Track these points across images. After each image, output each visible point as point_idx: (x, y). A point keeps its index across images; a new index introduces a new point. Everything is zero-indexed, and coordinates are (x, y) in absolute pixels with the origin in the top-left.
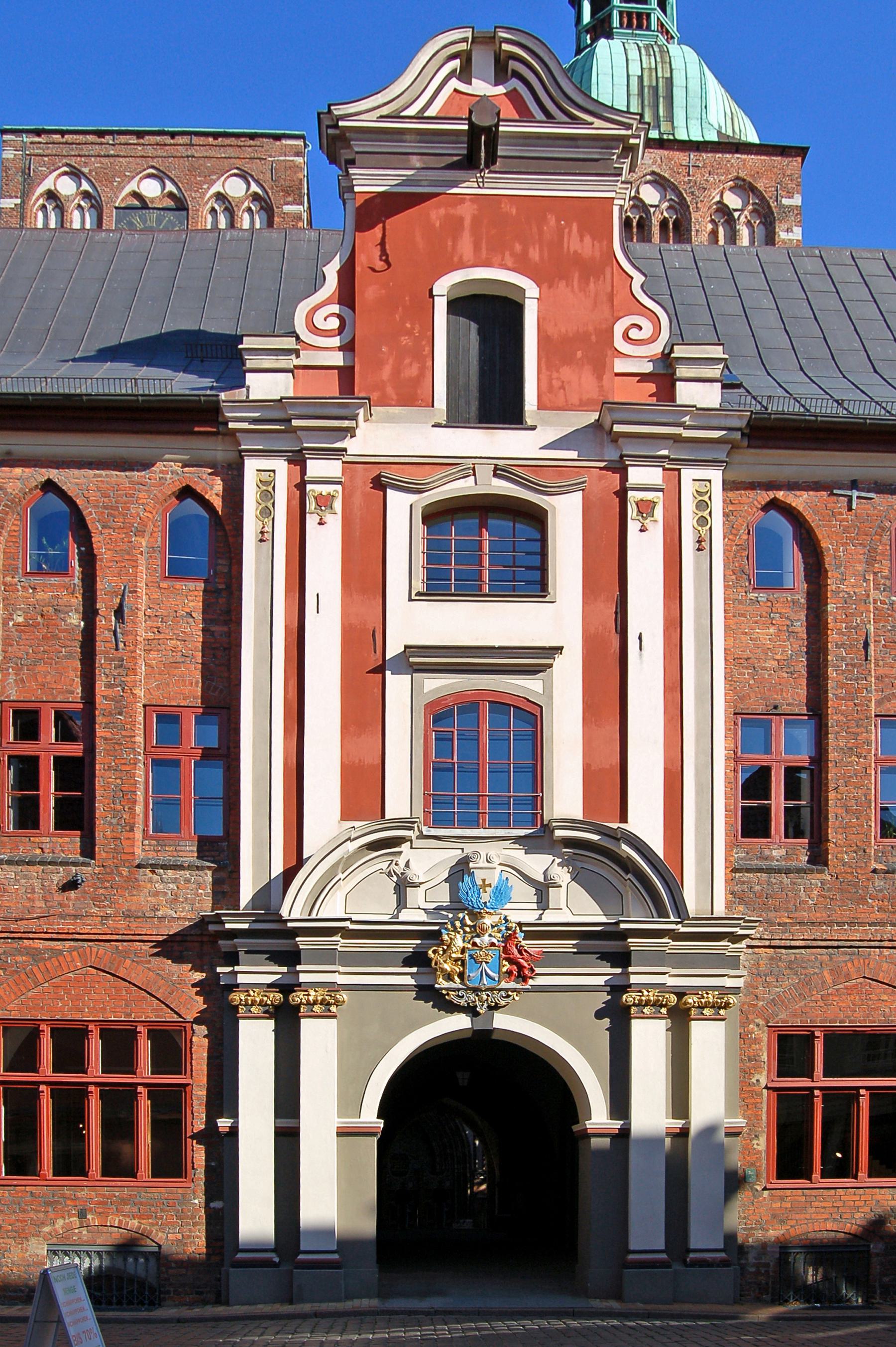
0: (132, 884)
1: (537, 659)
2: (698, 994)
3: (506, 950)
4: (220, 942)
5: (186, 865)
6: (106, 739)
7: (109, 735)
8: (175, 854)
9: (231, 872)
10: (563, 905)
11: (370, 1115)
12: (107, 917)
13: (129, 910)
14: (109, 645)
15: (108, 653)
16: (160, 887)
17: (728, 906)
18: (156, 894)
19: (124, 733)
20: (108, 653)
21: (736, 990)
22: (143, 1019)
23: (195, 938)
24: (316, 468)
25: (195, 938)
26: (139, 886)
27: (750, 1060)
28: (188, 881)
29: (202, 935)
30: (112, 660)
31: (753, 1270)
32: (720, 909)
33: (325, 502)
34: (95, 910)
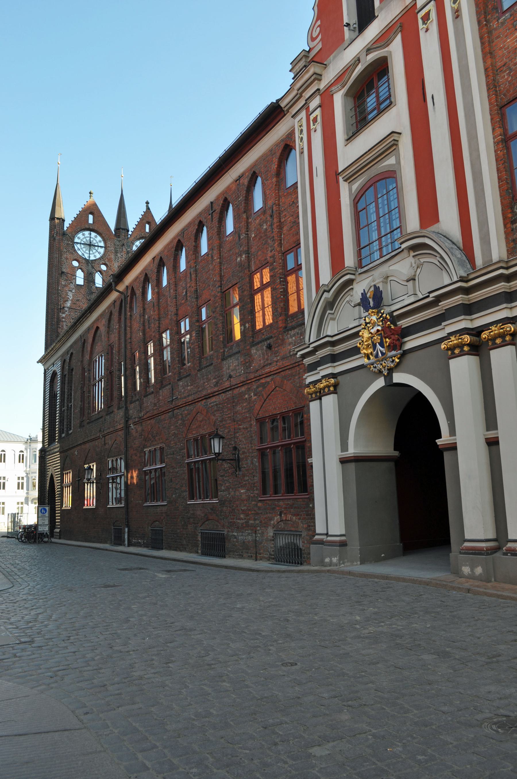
16: (290, 340)
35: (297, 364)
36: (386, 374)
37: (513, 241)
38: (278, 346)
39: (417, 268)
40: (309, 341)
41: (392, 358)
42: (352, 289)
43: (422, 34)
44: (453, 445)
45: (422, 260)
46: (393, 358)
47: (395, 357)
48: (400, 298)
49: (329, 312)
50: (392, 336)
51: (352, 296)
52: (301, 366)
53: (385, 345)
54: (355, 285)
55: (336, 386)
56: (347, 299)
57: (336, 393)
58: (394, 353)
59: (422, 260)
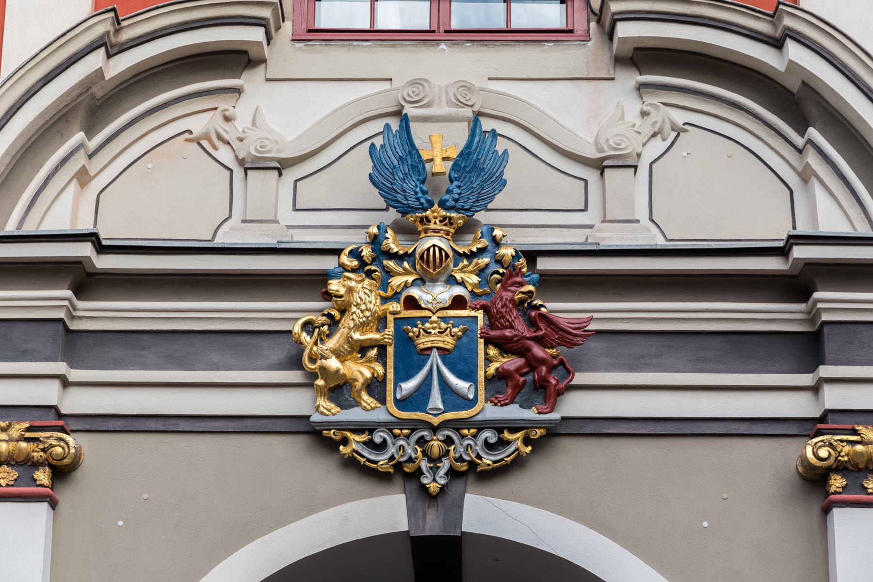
10: (642, 213)
36: (433, 487)
39: (654, 135)
42: (237, 91)
45: (680, 117)
46: (507, 435)
47: (513, 430)
48: (533, 211)
49: (80, 136)
50: (538, 351)
51: (227, 119)
53: (481, 374)
54: (251, 81)
55: (63, 471)
57: (54, 504)
58: (514, 412)
59: (680, 117)
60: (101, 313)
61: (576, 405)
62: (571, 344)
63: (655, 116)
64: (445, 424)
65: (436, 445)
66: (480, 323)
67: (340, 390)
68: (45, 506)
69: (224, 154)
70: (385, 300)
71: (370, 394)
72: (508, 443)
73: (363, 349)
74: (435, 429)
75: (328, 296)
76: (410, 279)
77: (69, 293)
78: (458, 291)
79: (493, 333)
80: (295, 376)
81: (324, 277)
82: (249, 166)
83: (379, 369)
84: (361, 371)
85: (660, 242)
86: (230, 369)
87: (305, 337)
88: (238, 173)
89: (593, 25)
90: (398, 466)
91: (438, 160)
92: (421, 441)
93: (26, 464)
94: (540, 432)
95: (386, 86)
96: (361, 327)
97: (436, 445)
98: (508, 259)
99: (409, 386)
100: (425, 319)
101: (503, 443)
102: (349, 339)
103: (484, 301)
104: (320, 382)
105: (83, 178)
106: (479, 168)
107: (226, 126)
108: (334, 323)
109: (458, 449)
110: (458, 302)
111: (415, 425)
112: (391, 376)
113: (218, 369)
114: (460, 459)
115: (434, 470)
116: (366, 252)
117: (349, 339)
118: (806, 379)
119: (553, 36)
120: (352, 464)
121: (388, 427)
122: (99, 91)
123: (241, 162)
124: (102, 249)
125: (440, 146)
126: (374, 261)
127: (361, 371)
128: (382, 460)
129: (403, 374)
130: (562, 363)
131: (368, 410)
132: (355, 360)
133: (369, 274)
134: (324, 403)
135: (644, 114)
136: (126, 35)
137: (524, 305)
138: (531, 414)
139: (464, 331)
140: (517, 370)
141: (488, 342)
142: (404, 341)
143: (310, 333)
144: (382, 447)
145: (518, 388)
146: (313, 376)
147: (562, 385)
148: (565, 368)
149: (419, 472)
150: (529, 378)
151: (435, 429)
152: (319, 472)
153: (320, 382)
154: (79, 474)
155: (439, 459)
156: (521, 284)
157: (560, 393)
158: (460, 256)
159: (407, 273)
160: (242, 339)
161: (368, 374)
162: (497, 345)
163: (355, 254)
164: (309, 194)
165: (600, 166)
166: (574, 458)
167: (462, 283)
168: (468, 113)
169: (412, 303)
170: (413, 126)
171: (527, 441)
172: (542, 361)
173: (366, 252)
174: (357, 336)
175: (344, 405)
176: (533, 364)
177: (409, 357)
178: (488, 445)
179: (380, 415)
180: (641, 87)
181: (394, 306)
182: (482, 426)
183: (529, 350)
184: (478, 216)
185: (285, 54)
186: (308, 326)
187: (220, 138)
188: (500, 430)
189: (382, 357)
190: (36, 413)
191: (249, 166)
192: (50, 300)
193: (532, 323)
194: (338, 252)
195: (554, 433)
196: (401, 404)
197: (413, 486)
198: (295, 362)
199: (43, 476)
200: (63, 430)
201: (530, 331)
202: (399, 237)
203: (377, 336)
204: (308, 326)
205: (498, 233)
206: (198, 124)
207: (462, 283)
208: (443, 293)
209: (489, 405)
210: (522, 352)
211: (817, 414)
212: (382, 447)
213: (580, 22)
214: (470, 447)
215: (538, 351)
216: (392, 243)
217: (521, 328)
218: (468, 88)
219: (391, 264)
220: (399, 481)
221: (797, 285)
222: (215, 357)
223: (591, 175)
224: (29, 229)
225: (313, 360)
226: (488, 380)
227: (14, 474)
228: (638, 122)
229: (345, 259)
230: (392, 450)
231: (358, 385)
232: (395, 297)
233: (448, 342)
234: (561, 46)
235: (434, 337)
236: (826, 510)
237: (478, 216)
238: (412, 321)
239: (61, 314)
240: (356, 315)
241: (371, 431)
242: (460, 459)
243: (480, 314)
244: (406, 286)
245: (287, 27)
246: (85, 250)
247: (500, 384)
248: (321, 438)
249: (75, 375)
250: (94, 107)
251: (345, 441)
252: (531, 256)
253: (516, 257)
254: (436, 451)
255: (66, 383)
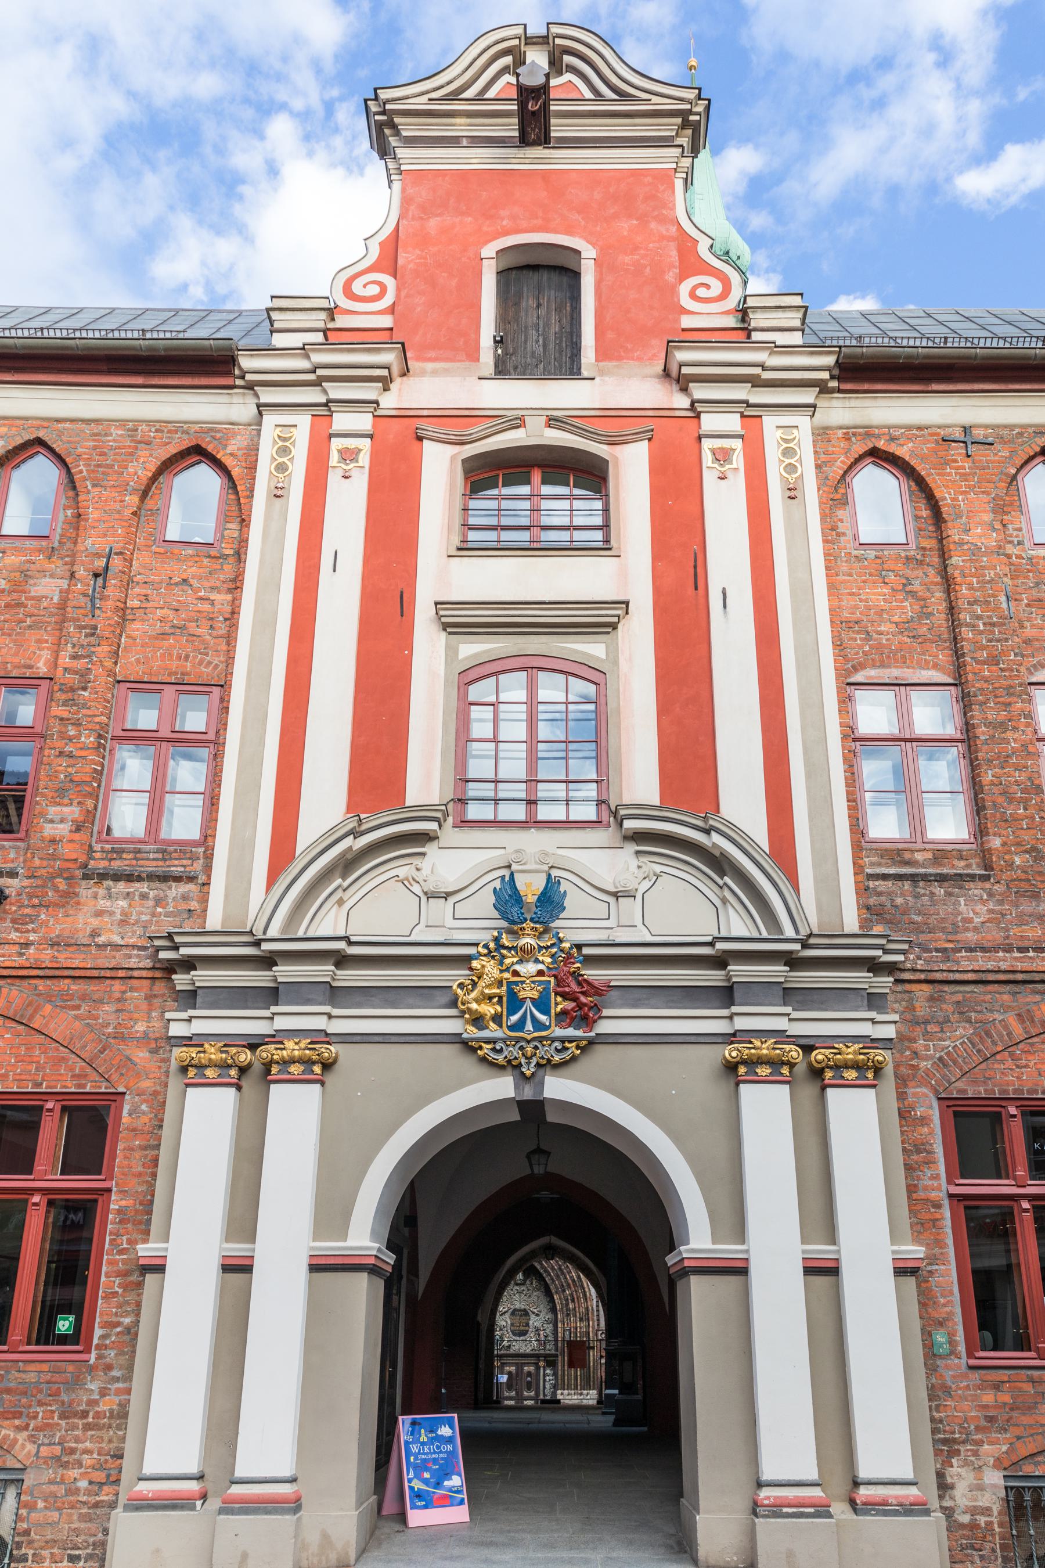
0: (68, 898)
1: (602, 620)
2: (834, 1048)
3: (559, 982)
4: (174, 977)
5: (144, 875)
6: (62, 719)
7: (65, 715)
8: (134, 862)
9: (204, 884)
11: (363, 1236)
12: (27, 945)
13: (58, 936)
14: (82, 611)
15: (78, 620)
16: (102, 903)
17: (864, 923)
18: (99, 913)
19: (85, 711)
20: (78, 620)
21: (886, 1043)
22: (58, 1090)
23: (144, 974)
24: (342, 421)
25: (144, 974)
26: (78, 903)
27: (919, 1151)
28: (144, 896)
29: (153, 968)
30: (84, 627)
31: (965, 1519)
32: (851, 922)
33: (349, 456)
34: (14, 936)
35: (121, 974)
36: (528, 1073)
37: (868, 908)
38: (41, 905)
40: (265, 933)
41: (563, 1042)
42: (423, 854)
43: (709, 478)
44: (247, 1262)
45: (658, 869)
46: (567, 1045)
47: (570, 1042)
49: (340, 880)
50: (583, 999)
51: (418, 869)
52: (135, 983)
53: (553, 1011)
55: (327, 1066)
56: (402, 872)
58: (570, 1032)
59: (658, 869)
60: (350, 977)
61: (605, 1027)
62: (600, 995)
63: (644, 869)
64: (534, 1039)
65: (529, 1050)
66: (552, 984)
67: (478, 1021)
68: (319, 1085)
69: (416, 888)
70: (501, 971)
71: (494, 1022)
72: (567, 1049)
73: (490, 998)
74: (528, 1042)
75: (471, 969)
76: (515, 960)
77: (333, 968)
78: (541, 967)
79: (559, 989)
80: (453, 1012)
81: (469, 958)
82: (430, 895)
83: (499, 1008)
84: (488, 1010)
85: (649, 939)
86: (419, 1007)
87: (459, 991)
88: (424, 899)
89: (612, 819)
90: (509, 1062)
91: (530, 896)
92: (522, 1048)
93: (309, 1062)
94: (584, 1043)
95: (502, 851)
96: (487, 986)
97: (529, 1050)
98: (567, 950)
99: (514, 1018)
100: (523, 982)
101: (566, 1049)
102: (482, 993)
103: (554, 972)
104: (467, 1016)
105: (340, 902)
106: (551, 900)
107: (417, 873)
108: (474, 984)
109: (540, 1052)
110: (540, 973)
111: (518, 1040)
112: (505, 1013)
113: (412, 1008)
114: (542, 1058)
115: (529, 1063)
116: (492, 945)
117: (482, 993)
118: (725, 1012)
119: (591, 825)
120: (484, 1060)
121: (504, 1040)
122: (349, 856)
123: (426, 893)
124: (350, 943)
125: (531, 886)
126: (496, 950)
127: (488, 1010)
128: (500, 1059)
129: (512, 1012)
130: (596, 1005)
131: (493, 1031)
132: (486, 1004)
133: (493, 957)
134: (471, 1028)
135: (639, 867)
136: (364, 827)
137: (576, 975)
138: (579, 1033)
139: (544, 989)
140: (572, 1009)
141: (556, 994)
142: (512, 995)
143: (462, 989)
144: (501, 1051)
145: (573, 1019)
146: (463, 1012)
147: (596, 1017)
148: (596, 1008)
149: (520, 1065)
150: (578, 1013)
151: (528, 1042)
152: (467, 1064)
153: (467, 1016)
154: (336, 1066)
155: (531, 1058)
156: (574, 963)
157: (595, 1021)
158: (541, 948)
159: (514, 956)
160: (426, 991)
161: (493, 1012)
162: (561, 996)
163: (486, 946)
164: (462, 910)
165: (616, 895)
166: (602, 1054)
167: (543, 962)
168: (546, 867)
169: (516, 973)
170: (516, 875)
171: (578, 1047)
172: (585, 1005)
173: (492, 945)
174: (487, 991)
175: (481, 1028)
176: (580, 1006)
177: (514, 1002)
178: (556, 1050)
179: (499, 1034)
180: (638, 853)
181: (507, 975)
182: (553, 1040)
183: (578, 998)
184: (552, 925)
185: (449, 834)
186: (461, 986)
187: (414, 880)
188: (563, 1042)
189: (500, 1002)
190: (314, 1034)
191: (430, 895)
192: (322, 971)
193: (579, 984)
194: (477, 945)
195: (591, 1042)
196: (511, 1028)
197: (517, 1072)
198: (454, 1003)
199: (317, 1069)
200: (329, 1043)
201: (579, 994)
202: (509, 936)
203: (497, 991)
204: (461, 986)
205: (561, 935)
206: (402, 872)
207: (543, 962)
208: (531, 968)
209: (557, 1028)
210: (575, 999)
211: (732, 1032)
212: (501, 1051)
213: (605, 816)
214: (547, 1051)
215: (583, 999)
216: (506, 941)
217: (574, 987)
218: (546, 854)
219: (504, 952)
220: (509, 1069)
221: (720, 961)
222: (411, 1001)
223: (611, 900)
224: (310, 934)
225: (463, 1004)
226: (557, 1015)
227: (302, 1068)
228: (636, 871)
229: (480, 949)
230: (506, 1053)
231: (487, 1018)
232: (507, 970)
233: (535, 995)
234: (594, 831)
235: (529, 992)
236: (737, 1084)
237: (552, 925)
238: (516, 983)
239: (328, 979)
240: (486, 980)
241: (495, 1043)
242: (542, 1058)
243: (552, 980)
244: (513, 964)
245: (450, 819)
246: (341, 945)
247: (563, 1017)
248: (468, 1046)
249: (336, 1012)
250: (347, 864)
251: (481, 1048)
252: (579, 947)
253: (571, 948)
254: (529, 1054)
255: (330, 1016)
